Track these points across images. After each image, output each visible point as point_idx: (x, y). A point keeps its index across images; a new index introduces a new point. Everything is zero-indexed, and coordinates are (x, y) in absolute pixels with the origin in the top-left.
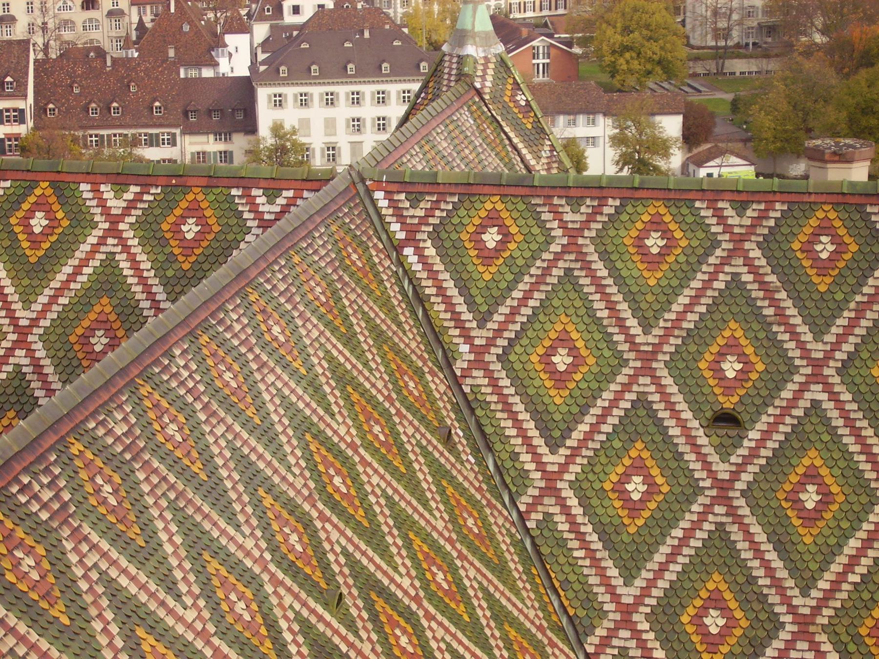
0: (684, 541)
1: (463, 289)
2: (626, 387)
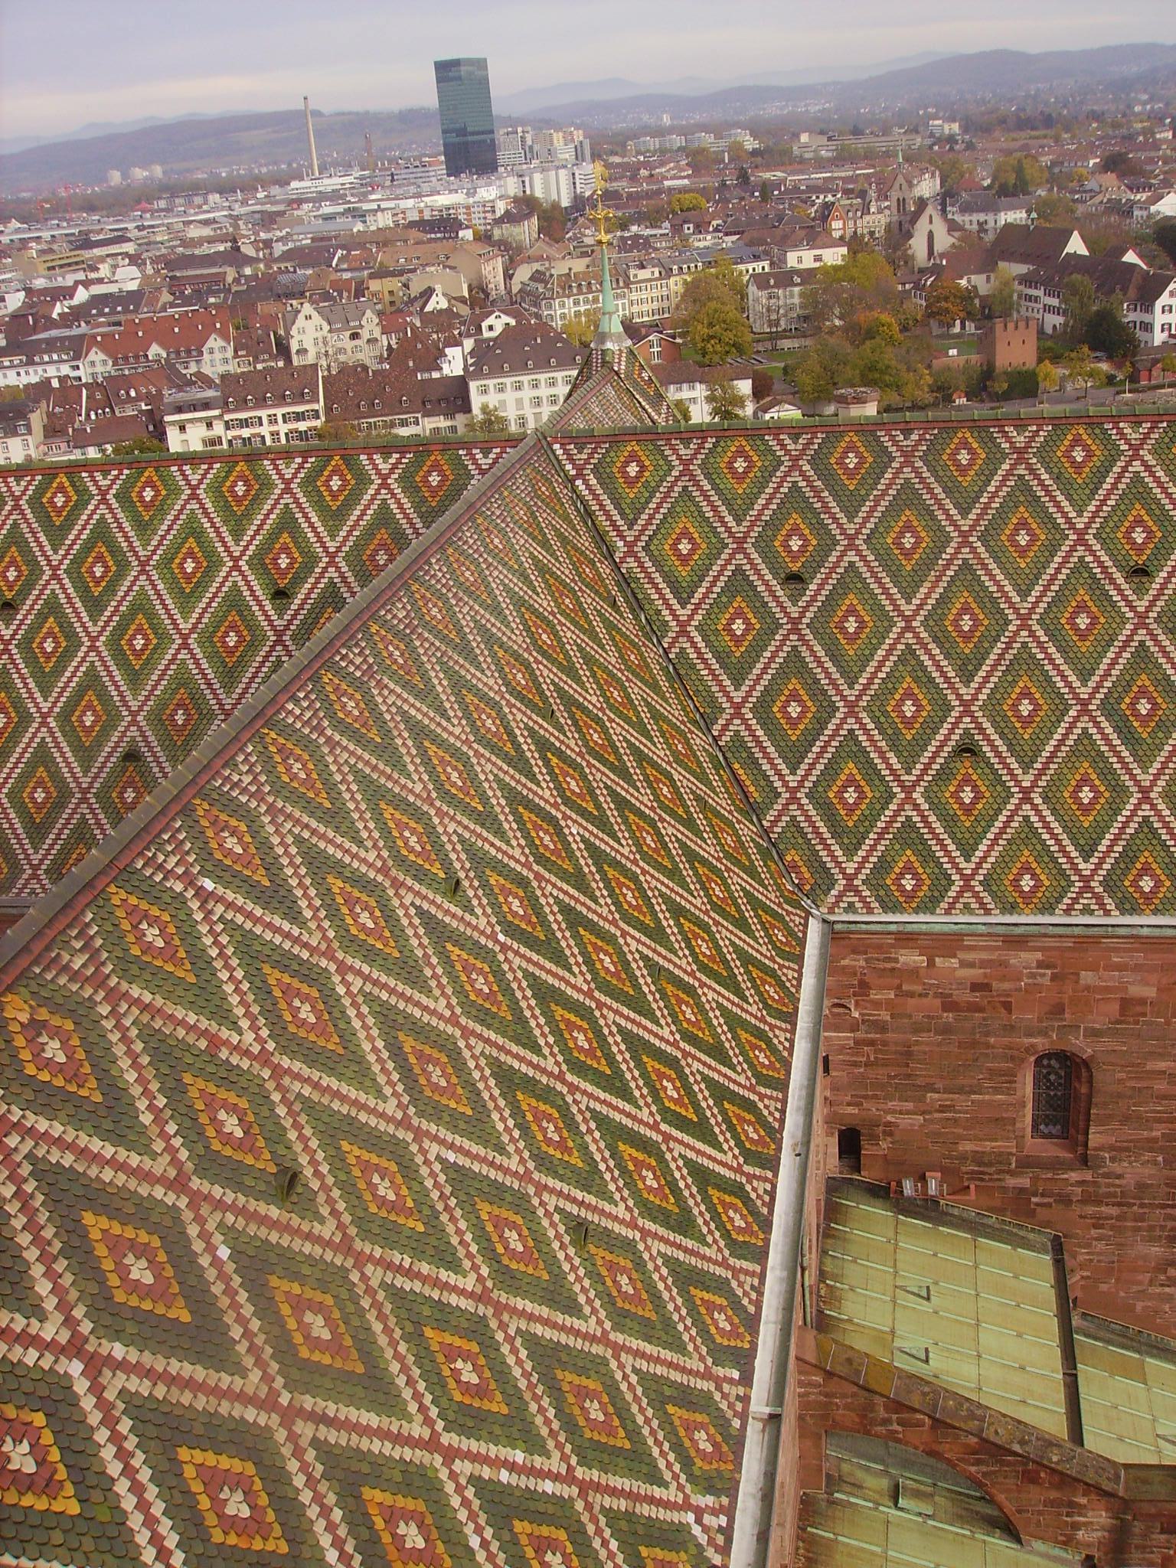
0: (772, 659)
1: (617, 505)
2: (728, 562)
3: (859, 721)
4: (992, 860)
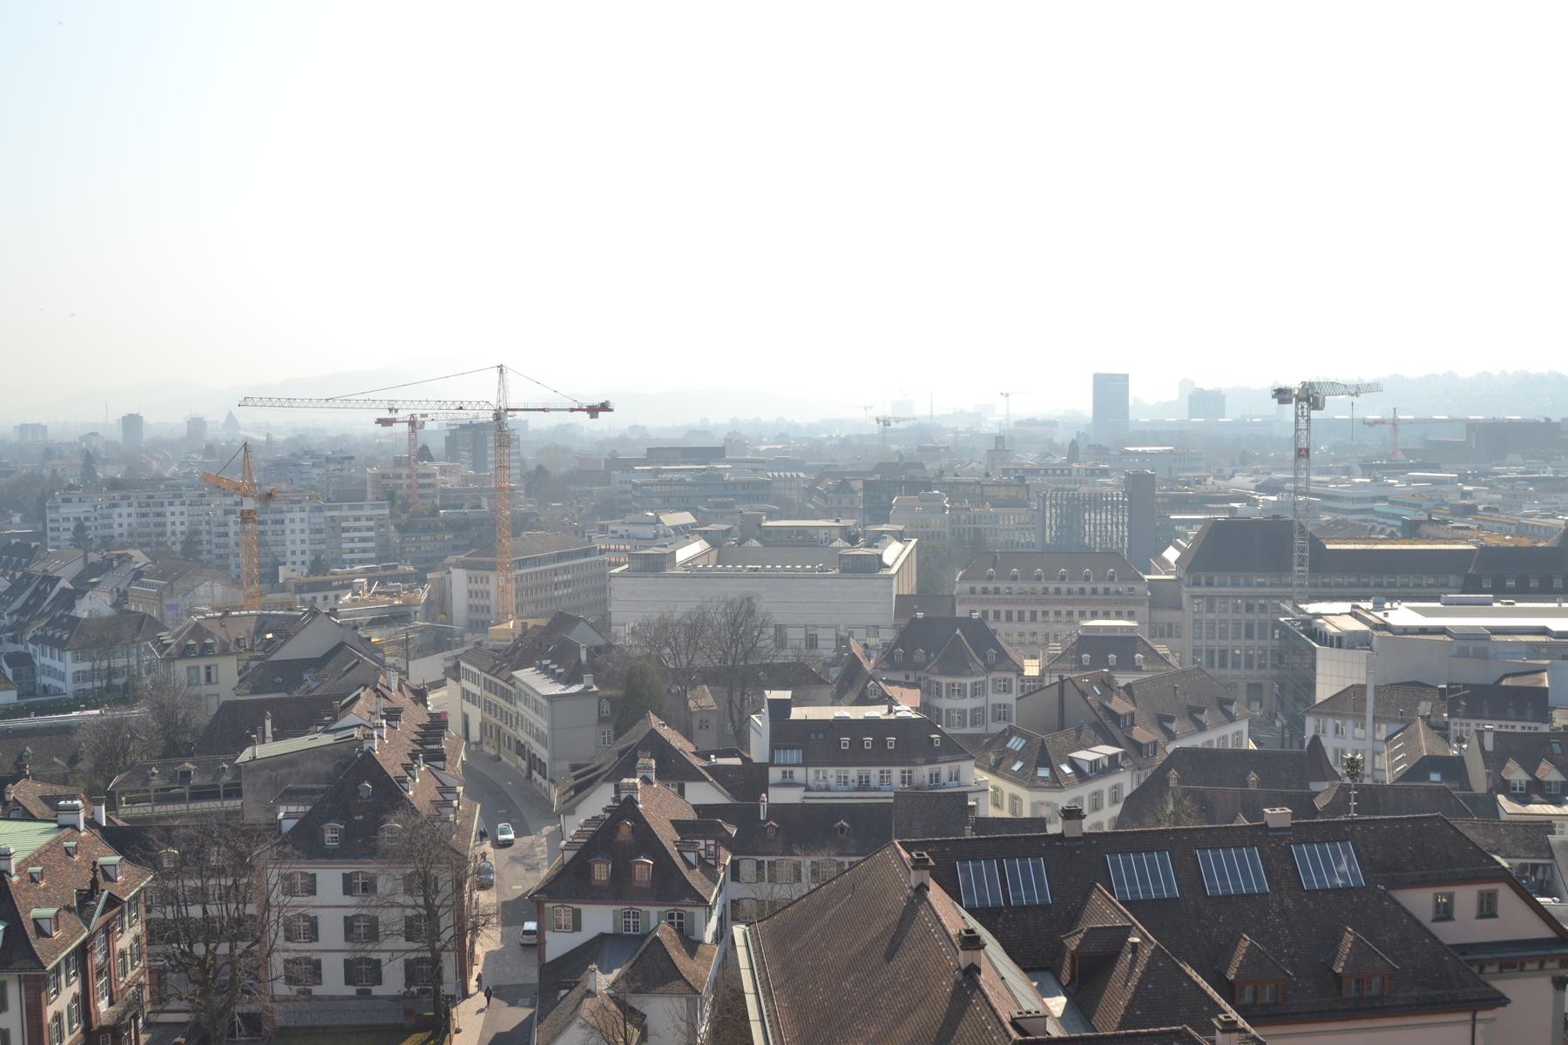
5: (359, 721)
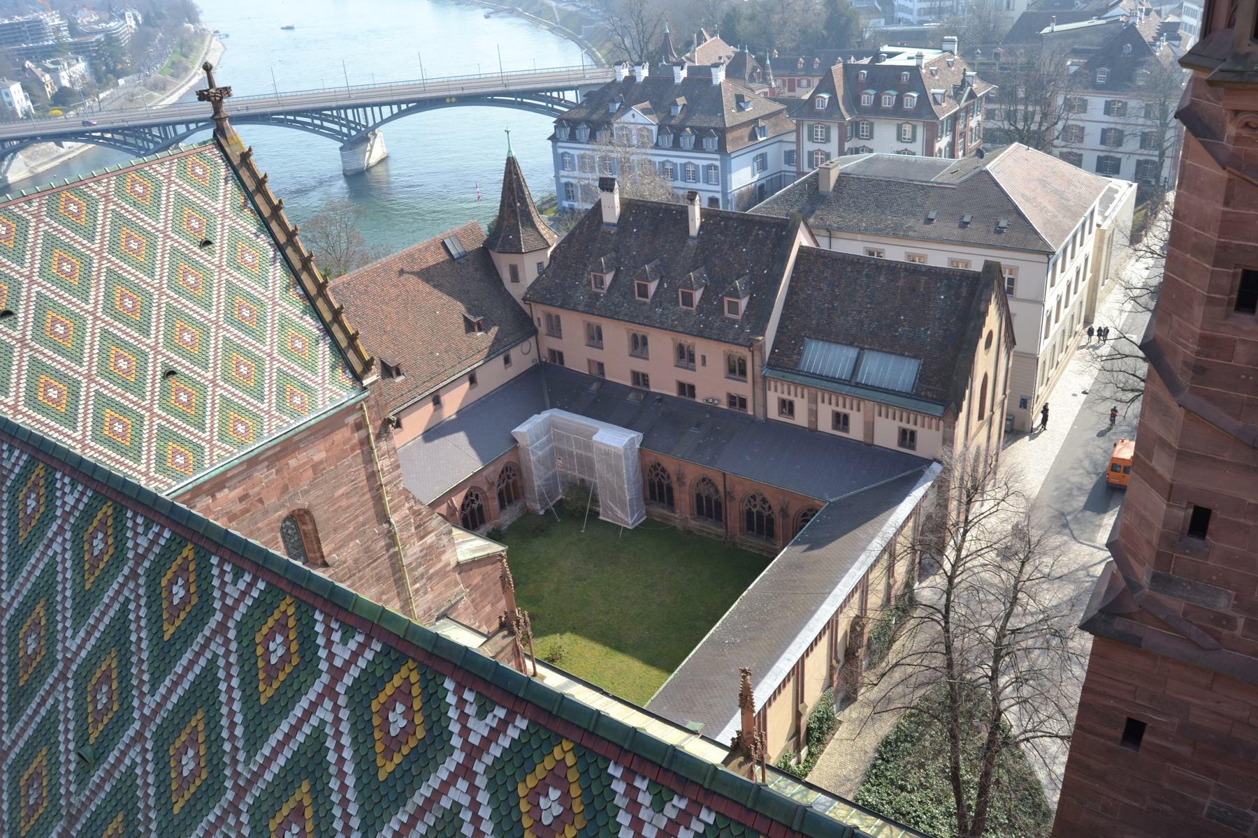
3: (97, 383)
4: (216, 425)
5: (1123, 12)
